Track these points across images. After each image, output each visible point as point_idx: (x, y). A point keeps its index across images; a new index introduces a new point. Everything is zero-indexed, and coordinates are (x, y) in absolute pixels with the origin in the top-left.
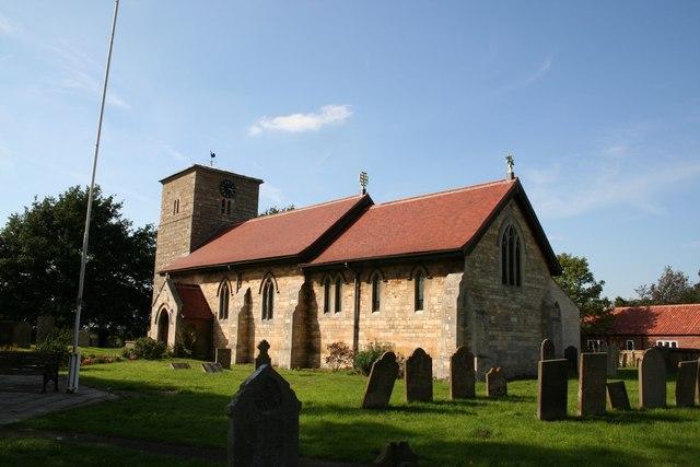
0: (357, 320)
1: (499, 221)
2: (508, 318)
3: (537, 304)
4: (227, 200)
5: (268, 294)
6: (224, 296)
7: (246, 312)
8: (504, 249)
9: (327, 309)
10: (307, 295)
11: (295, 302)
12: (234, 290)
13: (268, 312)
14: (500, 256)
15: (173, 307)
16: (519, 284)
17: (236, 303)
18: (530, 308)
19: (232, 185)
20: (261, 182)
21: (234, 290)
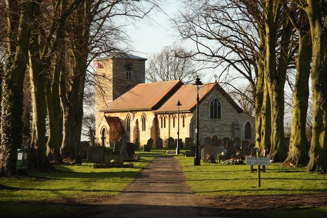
0: (169, 130)
1: (209, 98)
2: (213, 129)
3: (230, 123)
4: (129, 72)
5: (144, 120)
6: (129, 120)
7: (137, 128)
8: (212, 107)
9: (162, 127)
10: (156, 120)
11: (152, 125)
12: (132, 119)
13: (144, 129)
14: (210, 110)
15: (108, 127)
16: (219, 117)
17: (133, 125)
18: (225, 125)
19: (131, 65)
20: (146, 59)
21: (132, 119)
